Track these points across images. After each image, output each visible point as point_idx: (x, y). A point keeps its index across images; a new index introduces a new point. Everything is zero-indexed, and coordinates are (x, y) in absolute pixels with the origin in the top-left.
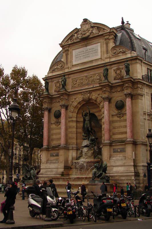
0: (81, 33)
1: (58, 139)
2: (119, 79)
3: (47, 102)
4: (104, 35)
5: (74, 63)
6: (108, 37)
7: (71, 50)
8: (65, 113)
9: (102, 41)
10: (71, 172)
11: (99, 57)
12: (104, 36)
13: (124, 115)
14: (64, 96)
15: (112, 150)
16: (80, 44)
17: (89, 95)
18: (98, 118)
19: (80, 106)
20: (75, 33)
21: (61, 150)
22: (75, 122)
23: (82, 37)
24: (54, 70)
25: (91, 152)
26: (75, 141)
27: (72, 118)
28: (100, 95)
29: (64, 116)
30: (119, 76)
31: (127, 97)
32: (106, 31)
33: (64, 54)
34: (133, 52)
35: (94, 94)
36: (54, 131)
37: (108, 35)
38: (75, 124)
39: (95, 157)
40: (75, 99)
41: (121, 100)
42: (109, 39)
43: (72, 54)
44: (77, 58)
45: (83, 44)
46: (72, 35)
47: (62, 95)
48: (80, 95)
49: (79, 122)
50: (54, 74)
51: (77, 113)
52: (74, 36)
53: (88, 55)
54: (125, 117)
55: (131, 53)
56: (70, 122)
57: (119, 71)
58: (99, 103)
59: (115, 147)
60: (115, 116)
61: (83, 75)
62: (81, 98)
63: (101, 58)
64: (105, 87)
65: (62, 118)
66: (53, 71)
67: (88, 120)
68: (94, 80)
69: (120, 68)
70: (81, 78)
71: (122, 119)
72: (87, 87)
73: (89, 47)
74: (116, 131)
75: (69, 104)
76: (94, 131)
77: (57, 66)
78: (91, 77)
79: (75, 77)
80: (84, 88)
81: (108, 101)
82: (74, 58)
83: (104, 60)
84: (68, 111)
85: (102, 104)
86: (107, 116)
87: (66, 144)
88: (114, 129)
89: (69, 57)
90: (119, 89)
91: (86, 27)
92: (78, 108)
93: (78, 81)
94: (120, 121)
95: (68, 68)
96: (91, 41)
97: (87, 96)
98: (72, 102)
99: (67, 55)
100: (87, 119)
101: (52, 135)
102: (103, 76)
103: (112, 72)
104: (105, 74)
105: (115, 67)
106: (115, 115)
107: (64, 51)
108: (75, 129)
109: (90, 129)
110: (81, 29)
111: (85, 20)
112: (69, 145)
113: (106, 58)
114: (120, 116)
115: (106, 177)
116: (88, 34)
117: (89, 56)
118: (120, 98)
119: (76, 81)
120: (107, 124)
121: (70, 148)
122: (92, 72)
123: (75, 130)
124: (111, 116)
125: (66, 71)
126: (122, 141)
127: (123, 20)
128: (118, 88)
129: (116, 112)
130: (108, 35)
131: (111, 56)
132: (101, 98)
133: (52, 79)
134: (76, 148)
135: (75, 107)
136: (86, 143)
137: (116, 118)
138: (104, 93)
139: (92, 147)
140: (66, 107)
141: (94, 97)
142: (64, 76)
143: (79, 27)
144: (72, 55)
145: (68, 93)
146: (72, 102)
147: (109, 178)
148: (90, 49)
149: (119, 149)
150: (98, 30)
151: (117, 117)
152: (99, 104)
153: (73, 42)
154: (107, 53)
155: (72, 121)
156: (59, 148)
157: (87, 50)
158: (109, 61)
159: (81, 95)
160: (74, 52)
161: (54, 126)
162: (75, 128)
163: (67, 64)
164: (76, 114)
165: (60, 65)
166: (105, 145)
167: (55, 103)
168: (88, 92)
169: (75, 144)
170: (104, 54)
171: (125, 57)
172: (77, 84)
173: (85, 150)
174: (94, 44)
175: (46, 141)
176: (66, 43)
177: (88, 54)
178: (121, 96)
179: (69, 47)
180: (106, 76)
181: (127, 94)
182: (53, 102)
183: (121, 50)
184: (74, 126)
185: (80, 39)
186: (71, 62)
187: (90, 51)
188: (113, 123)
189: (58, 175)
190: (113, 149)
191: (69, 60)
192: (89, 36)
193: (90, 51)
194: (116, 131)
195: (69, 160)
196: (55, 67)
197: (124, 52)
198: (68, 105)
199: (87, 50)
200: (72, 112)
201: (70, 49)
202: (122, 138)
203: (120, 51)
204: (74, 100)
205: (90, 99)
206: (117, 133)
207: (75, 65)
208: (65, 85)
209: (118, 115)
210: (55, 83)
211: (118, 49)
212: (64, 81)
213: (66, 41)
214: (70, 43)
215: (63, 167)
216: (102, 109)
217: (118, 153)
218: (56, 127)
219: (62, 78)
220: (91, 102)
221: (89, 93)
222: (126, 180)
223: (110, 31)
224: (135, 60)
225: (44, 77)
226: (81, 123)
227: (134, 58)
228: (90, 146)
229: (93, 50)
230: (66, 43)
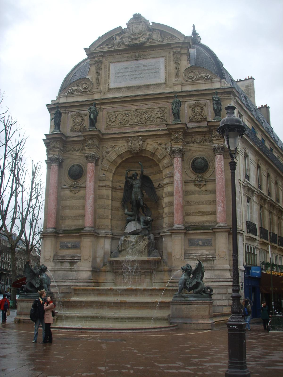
0: (129, 37)
1: (76, 216)
2: (198, 122)
3: (59, 148)
4: (172, 46)
5: (112, 86)
6: (179, 50)
7: (107, 62)
8: (94, 172)
9: (168, 56)
10: (102, 278)
11: (161, 80)
12: (172, 48)
13: (207, 183)
14: (95, 140)
15: (187, 242)
16: (126, 55)
17: (141, 143)
18: (154, 184)
19: (120, 162)
20: (117, 35)
22: (111, 189)
23: (131, 43)
24: (72, 93)
25: (143, 244)
26: (107, 222)
27: (104, 180)
28: (163, 146)
29: (93, 178)
30: (200, 117)
31: (218, 152)
32: (177, 39)
33: (93, 68)
34: (223, 80)
35: (151, 143)
36: (68, 203)
37: (179, 47)
38: (110, 192)
39: (149, 254)
40: (113, 148)
41: (204, 158)
42: (181, 54)
43: (109, 70)
44: (118, 76)
46: (112, 37)
47: (92, 137)
49: (116, 189)
50: (71, 100)
51: (114, 174)
52: (116, 39)
53: (141, 76)
54: (209, 187)
55: (220, 82)
56: (101, 188)
57: (199, 109)
58: (161, 158)
59: (192, 237)
60: (189, 184)
61: (128, 108)
62: (124, 148)
63: (165, 84)
64: (176, 132)
65: (88, 179)
66: (69, 95)
67: (139, 187)
68: (151, 119)
69: (201, 104)
70: (126, 112)
71: (203, 189)
72: (136, 129)
73: (141, 62)
74: (193, 209)
75: (100, 155)
76: (147, 207)
77: (78, 86)
78: (146, 113)
79: (115, 110)
81: (181, 156)
82: (112, 77)
83: (170, 87)
84: (99, 167)
85: (165, 161)
86: (180, 182)
87: (93, 227)
88: (189, 207)
89: (102, 73)
90: (199, 138)
91: (138, 27)
92: (117, 165)
93: (119, 117)
94: (200, 193)
95: (101, 93)
96: (146, 53)
97: (138, 144)
98: (107, 153)
99: (98, 70)
100: (138, 185)
101: (64, 208)
102: (173, 112)
103: (186, 109)
104: (177, 111)
105: (191, 101)
106: (191, 182)
107: (94, 63)
108: (110, 201)
109: (142, 203)
110: (128, 30)
111: (137, 18)
112: (98, 229)
113: (175, 85)
114: (200, 185)
115: (206, 290)
116: (142, 40)
117: (142, 78)
118: (201, 153)
119: (116, 117)
120: (180, 197)
121: (100, 235)
122: (147, 105)
123: (109, 202)
124: (184, 183)
125: (96, 97)
126: (202, 227)
127: (194, 29)
128: (196, 136)
129: (193, 176)
130: (179, 47)
131: (184, 82)
132: (163, 150)
133: (66, 108)
134: (111, 236)
135: (112, 162)
136: (132, 227)
137: (192, 187)
138: (176, 142)
139: (146, 235)
140: (96, 160)
141: (149, 148)
142: (95, 105)
143: (124, 26)
144: (109, 72)
145: (101, 136)
146: (107, 153)
147: (212, 291)
148: (144, 66)
149: (201, 240)
150: (161, 36)
151: (193, 186)
152: (160, 160)
153: (112, 49)
155: (105, 186)
156: (82, 234)
157: (139, 67)
158: (180, 90)
159: (125, 141)
160: (112, 66)
161: (67, 193)
162: (109, 199)
163: (98, 85)
164: (112, 174)
165: (84, 86)
166: (173, 232)
167: (70, 152)
168: (140, 138)
169: (110, 227)
170: (170, 77)
172: (118, 122)
173: (133, 239)
174: (153, 58)
175: (53, 220)
176: (97, 49)
177: (140, 74)
178: (202, 151)
179: (103, 56)
180: (177, 115)
181: (219, 148)
182: (68, 149)
183: (204, 75)
184: (108, 196)
185: (128, 46)
186: (107, 82)
187: (145, 68)
188: (185, 195)
189: (81, 284)
190: (189, 240)
191: (102, 79)
192: (144, 43)
193: (145, 68)
194: (193, 209)
195: (97, 256)
196: (74, 88)
197: (209, 79)
198: (99, 157)
199: (139, 67)
200: (107, 170)
201: (104, 60)
202: (203, 222)
203: (202, 77)
204: (110, 149)
205: (142, 150)
206: (193, 212)
207: (115, 90)
208: (96, 122)
209: (197, 183)
210: (72, 116)
211: (197, 72)
212: (94, 113)
213: (99, 46)
214: (106, 49)
215: (89, 269)
216: (164, 169)
217: (198, 248)
218: (72, 194)
219: (90, 108)
220: (143, 155)
221: (141, 140)
222: (218, 294)
223: (184, 40)
224: (228, 94)
225: (50, 103)
226: (121, 191)
227: (227, 90)
228: (140, 232)
229: (151, 67)
230: (98, 50)
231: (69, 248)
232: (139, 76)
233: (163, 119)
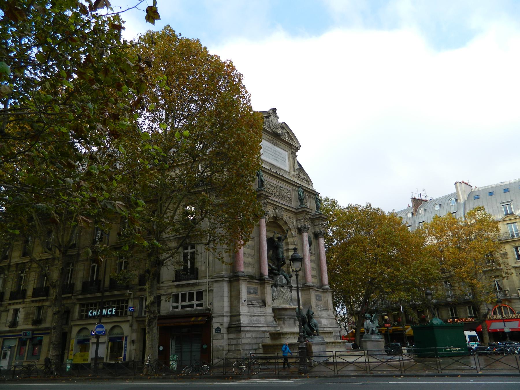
4: (292, 147)
12: (291, 148)
16: (268, 137)
21: (268, 285)
45: (270, 138)
48: (271, 208)
53: (277, 159)
61: (271, 181)
62: (272, 213)
72: (277, 200)
73: (276, 148)
80: (274, 199)
96: (278, 142)
111: (274, 110)
117: (278, 161)
154: (294, 171)
171: (307, 186)
185: (274, 132)
187: (278, 154)
193: (278, 154)
231: (251, 293)
232: (276, 158)
233: (290, 201)
